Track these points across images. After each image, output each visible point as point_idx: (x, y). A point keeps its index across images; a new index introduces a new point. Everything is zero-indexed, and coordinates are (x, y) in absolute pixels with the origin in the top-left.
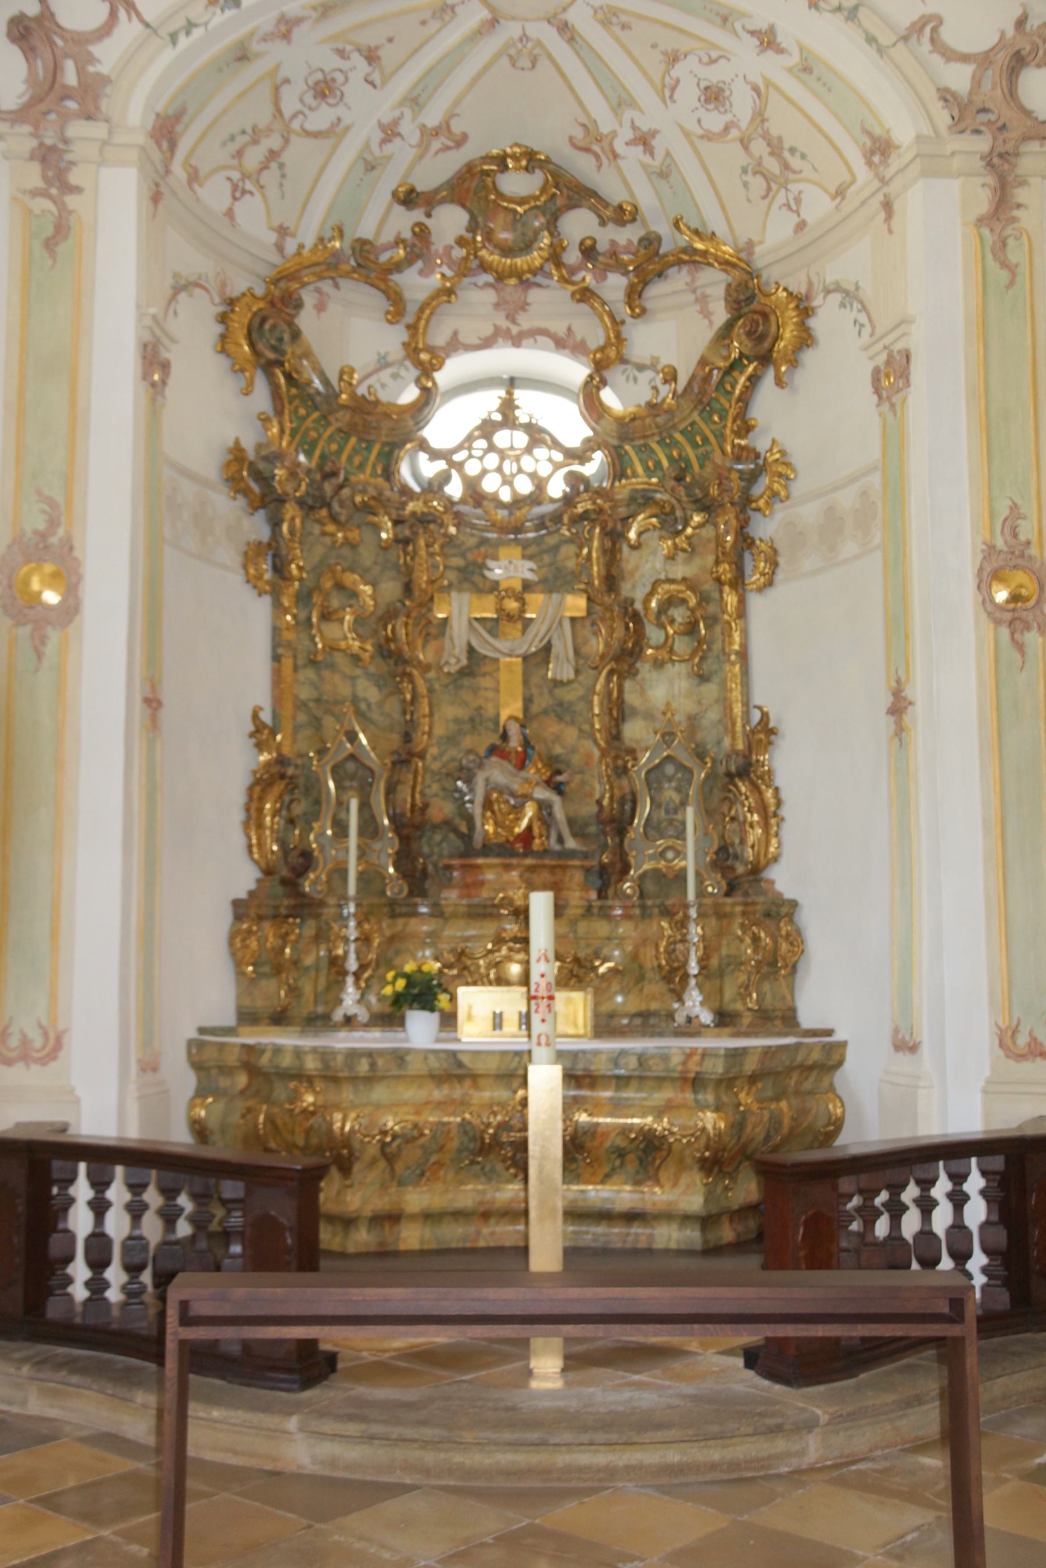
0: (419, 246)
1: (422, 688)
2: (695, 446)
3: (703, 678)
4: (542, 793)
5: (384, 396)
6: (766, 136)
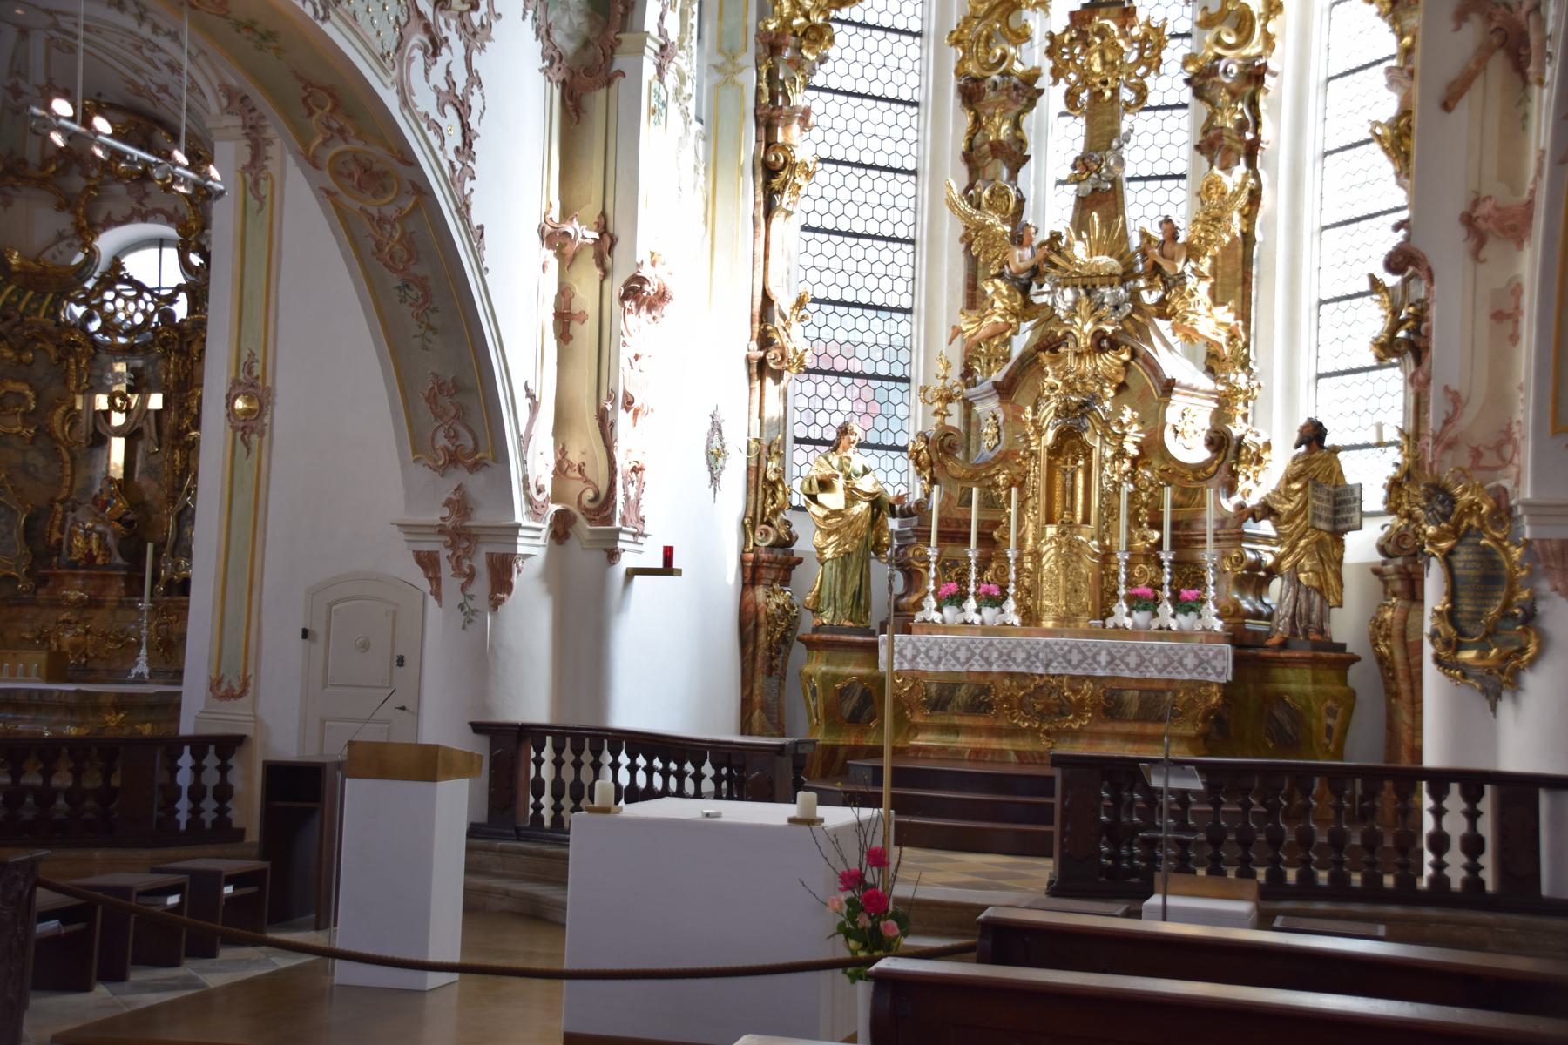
5: (60, 260)
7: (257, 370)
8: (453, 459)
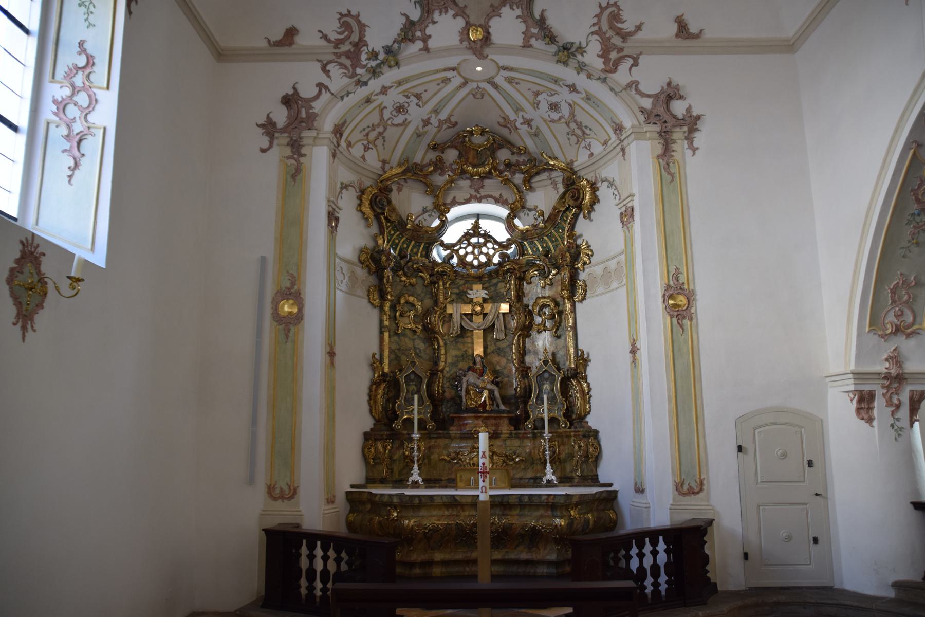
0: (439, 165)
1: (442, 343)
2: (552, 242)
3: (559, 337)
4: (490, 386)
5: (425, 224)
6: (575, 121)
7: (683, 279)
8: (897, 330)
